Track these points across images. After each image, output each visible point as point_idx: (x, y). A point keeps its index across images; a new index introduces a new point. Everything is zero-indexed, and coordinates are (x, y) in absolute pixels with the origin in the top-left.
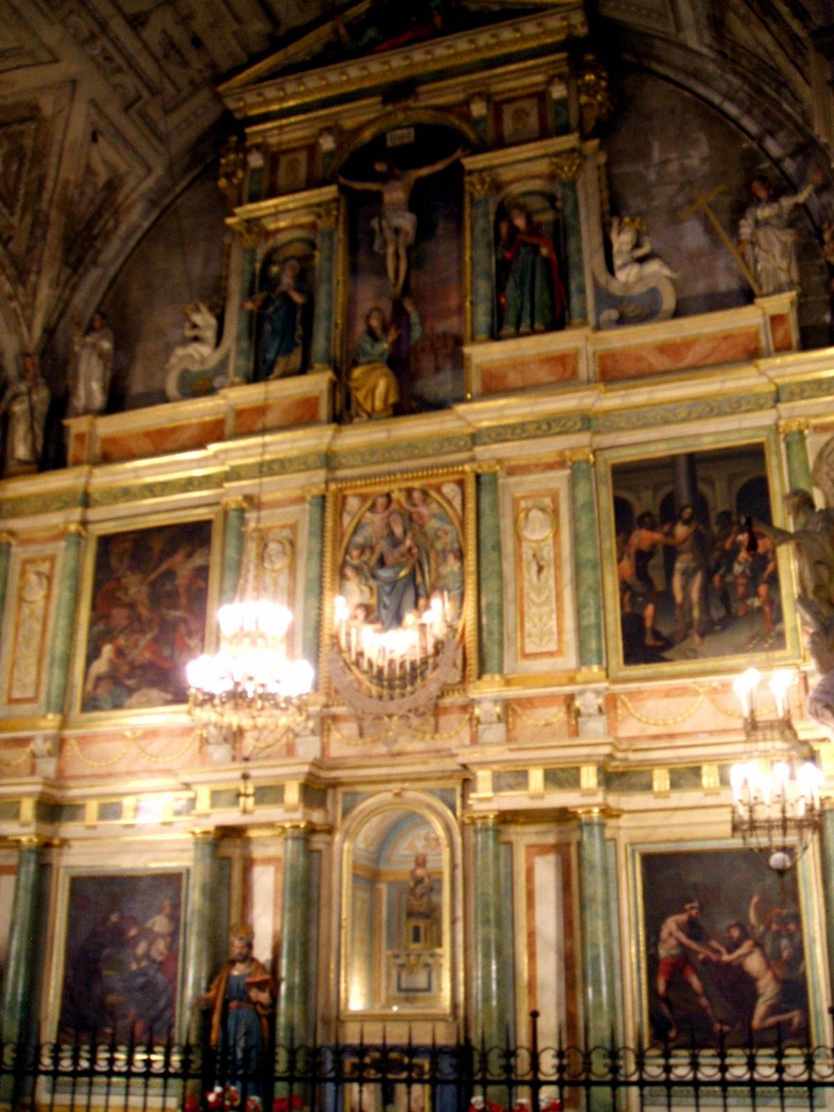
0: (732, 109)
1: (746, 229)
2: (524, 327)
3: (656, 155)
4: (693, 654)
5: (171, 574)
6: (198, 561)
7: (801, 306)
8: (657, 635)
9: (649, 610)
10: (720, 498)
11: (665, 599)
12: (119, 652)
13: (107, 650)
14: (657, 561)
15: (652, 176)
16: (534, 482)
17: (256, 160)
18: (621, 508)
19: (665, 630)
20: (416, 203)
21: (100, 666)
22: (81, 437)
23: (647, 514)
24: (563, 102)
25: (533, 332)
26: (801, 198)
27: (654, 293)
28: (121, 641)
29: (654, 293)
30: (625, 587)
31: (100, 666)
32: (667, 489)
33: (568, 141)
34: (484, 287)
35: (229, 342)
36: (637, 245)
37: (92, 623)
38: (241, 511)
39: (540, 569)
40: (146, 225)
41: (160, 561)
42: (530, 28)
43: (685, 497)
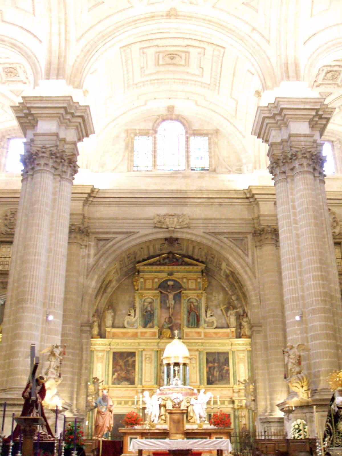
0: (227, 289)
1: (229, 314)
2: (193, 326)
3: (214, 294)
4: (217, 384)
5: (128, 361)
6: (133, 359)
7: (236, 330)
8: (212, 380)
9: (211, 377)
10: (222, 360)
11: (213, 375)
12: (119, 374)
13: (116, 374)
14: (212, 369)
15: (213, 299)
18: (207, 359)
19: (213, 380)
20: (174, 298)
21: (115, 376)
22: (109, 332)
23: (211, 361)
24: (199, 282)
25: (194, 328)
26: (237, 310)
27: (213, 322)
28: (119, 372)
29: (213, 322)
30: (207, 372)
32: (214, 357)
33: (201, 291)
34: (185, 317)
35: (136, 317)
36: (211, 313)
37: (113, 368)
38: (142, 351)
39: (194, 368)
40: (116, 287)
41: (125, 359)
42: (195, 268)
43: (217, 359)
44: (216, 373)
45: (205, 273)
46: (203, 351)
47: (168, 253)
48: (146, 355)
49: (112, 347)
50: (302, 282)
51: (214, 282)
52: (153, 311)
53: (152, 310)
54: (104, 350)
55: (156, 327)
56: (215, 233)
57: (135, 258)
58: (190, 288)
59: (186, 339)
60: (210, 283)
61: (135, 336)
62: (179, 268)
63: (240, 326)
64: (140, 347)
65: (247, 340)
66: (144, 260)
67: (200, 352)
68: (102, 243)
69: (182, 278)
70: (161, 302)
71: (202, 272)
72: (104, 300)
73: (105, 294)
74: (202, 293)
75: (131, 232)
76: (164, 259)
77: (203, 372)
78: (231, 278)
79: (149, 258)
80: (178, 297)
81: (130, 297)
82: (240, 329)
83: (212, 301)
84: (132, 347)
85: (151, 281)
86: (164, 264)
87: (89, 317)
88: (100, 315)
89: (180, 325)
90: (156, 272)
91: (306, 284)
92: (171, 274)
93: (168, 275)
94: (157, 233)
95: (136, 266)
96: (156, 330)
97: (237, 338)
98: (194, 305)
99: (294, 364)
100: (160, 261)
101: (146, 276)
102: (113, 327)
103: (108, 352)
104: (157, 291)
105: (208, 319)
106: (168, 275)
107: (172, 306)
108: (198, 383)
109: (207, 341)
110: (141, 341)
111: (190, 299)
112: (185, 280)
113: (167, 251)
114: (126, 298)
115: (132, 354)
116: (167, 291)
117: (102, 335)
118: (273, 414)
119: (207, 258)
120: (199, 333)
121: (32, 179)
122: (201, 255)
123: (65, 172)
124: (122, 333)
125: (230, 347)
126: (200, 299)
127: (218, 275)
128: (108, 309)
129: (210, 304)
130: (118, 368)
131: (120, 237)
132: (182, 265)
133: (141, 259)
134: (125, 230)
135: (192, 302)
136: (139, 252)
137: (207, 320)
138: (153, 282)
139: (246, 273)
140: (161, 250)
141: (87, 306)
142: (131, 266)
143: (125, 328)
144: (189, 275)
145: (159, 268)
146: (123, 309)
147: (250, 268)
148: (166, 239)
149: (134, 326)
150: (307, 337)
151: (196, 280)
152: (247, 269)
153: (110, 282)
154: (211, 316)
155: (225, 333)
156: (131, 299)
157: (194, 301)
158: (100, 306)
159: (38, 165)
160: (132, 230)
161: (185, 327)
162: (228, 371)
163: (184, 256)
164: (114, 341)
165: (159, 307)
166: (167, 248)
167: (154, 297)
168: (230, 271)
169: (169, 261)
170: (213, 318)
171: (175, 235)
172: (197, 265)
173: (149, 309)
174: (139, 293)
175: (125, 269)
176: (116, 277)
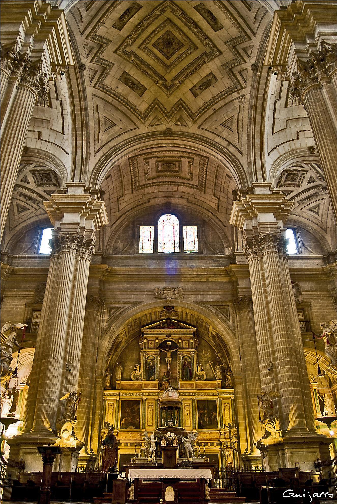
5: (134, 408)
10: (211, 407)
12: (126, 420)
16: (187, 401)
17: (146, 341)
20: (171, 356)
21: (123, 422)
24: (192, 342)
31: (123, 422)
33: (193, 350)
35: (141, 372)
44: (206, 419)
45: (196, 335)
46: (195, 400)
47: (167, 319)
48: (148, 403)
49: (121, 397)
50: (272, 340)
51: (203, 342)
52: (155, 367)
53: (154, 365)
54: (115, 400)
55: (157, 380)
56: (203, 303)
57: (140, 323)
58: (184, 347)
59: (181, 390)
60: (200, 343)
61: (140, 387)
62: (175, 331)
63: (224, 379)
64: (144, 397)
65: (231, 391)
66: (147, 325)
67: (193, 401)
68: (113, 311)
69: (178, 339)
70: (161, 359)
71: (194, 334)
72: (114, 358)
73: (117, 353)
74: (194, 351)
75: (136, 302)
76: (163, 323)
77: (195, 418)
78: (217, 339)
79: (151, 324)
80: (174, 356)
81: (136, 355)
82: (225, 381)
83: (202, 358)
84: (137, 397)
85: (153, 342)
86: (164, 328)
87: (102, 371)
88: (112, 370)
89: (176, 378)
90: (157, 334)
91: (275, 342)
92: (169, 335)
93: (167, 337)
94: (157, 303)
95: (141, 330)
96: (157, 382)
97: (222, 388)
98: (187, 361)
99: (267, 408)
100: (160, 325)
101: (150, 337)
102: (122, 379)
103: (118, 401)
104: (158, 350)
105: (199, 373)
106: (167, 337)
107: (170, 363)
108: (192, 428)
109: (198, 391)
110: (145, 391)
111: (184, 356)
112: (180, 341)
113: (167, 317)
114: (133, 356)
115: (138, 403)
116: (165, 350)
117: (113, 387)
118: (253, 453)
119: (197, 323)
120: (192, 385)
121: (58, 259)
122: (193, 320)
123: (84, 253)
124: (129, 385)
125: (217, 397)
126: (193, 357)
127: (207, 337)
128: (119, 365)
129: (200, 360)
130: (126, 414)
131: (128, 305)
132: (177, 328)
133: (145, 324)
134: (132, 300)
135: (186, 359)
136: (143, 318)
137: (198, 374)
138: (154, 343)
139: (229, 335)
140: (161, 316)
141: (101, 362)
142: (137, 329)
143: (132, 380)
144: (184, 337)
145: (159, 331)
146: (130, 365)
147: (231, 330)
148: (164, 307)
149: (139, 379)
150: (277, 385)
151: (189, 341)
152: (229, 331)
153: (120, 342)
154: (201, 370)
155: (213, 384)
156: (137, 357)
157: (188, 358)
158: (111, 364)
159: (63, 247)
160: (138, 300)
161: (180, 379)
162: (216, 416)
163: (179, 321)
164: (123, 391)
165: (159, 363)
166: (165, 315)
167: (155, 355)
168: (216, 333)
169: (168, 326)
170: (203, 371)
171: (171, 305)
172: (190, 328)
173: (151, 364)
174: (144, 352)
175: (132, 332)
176: (126, 338)
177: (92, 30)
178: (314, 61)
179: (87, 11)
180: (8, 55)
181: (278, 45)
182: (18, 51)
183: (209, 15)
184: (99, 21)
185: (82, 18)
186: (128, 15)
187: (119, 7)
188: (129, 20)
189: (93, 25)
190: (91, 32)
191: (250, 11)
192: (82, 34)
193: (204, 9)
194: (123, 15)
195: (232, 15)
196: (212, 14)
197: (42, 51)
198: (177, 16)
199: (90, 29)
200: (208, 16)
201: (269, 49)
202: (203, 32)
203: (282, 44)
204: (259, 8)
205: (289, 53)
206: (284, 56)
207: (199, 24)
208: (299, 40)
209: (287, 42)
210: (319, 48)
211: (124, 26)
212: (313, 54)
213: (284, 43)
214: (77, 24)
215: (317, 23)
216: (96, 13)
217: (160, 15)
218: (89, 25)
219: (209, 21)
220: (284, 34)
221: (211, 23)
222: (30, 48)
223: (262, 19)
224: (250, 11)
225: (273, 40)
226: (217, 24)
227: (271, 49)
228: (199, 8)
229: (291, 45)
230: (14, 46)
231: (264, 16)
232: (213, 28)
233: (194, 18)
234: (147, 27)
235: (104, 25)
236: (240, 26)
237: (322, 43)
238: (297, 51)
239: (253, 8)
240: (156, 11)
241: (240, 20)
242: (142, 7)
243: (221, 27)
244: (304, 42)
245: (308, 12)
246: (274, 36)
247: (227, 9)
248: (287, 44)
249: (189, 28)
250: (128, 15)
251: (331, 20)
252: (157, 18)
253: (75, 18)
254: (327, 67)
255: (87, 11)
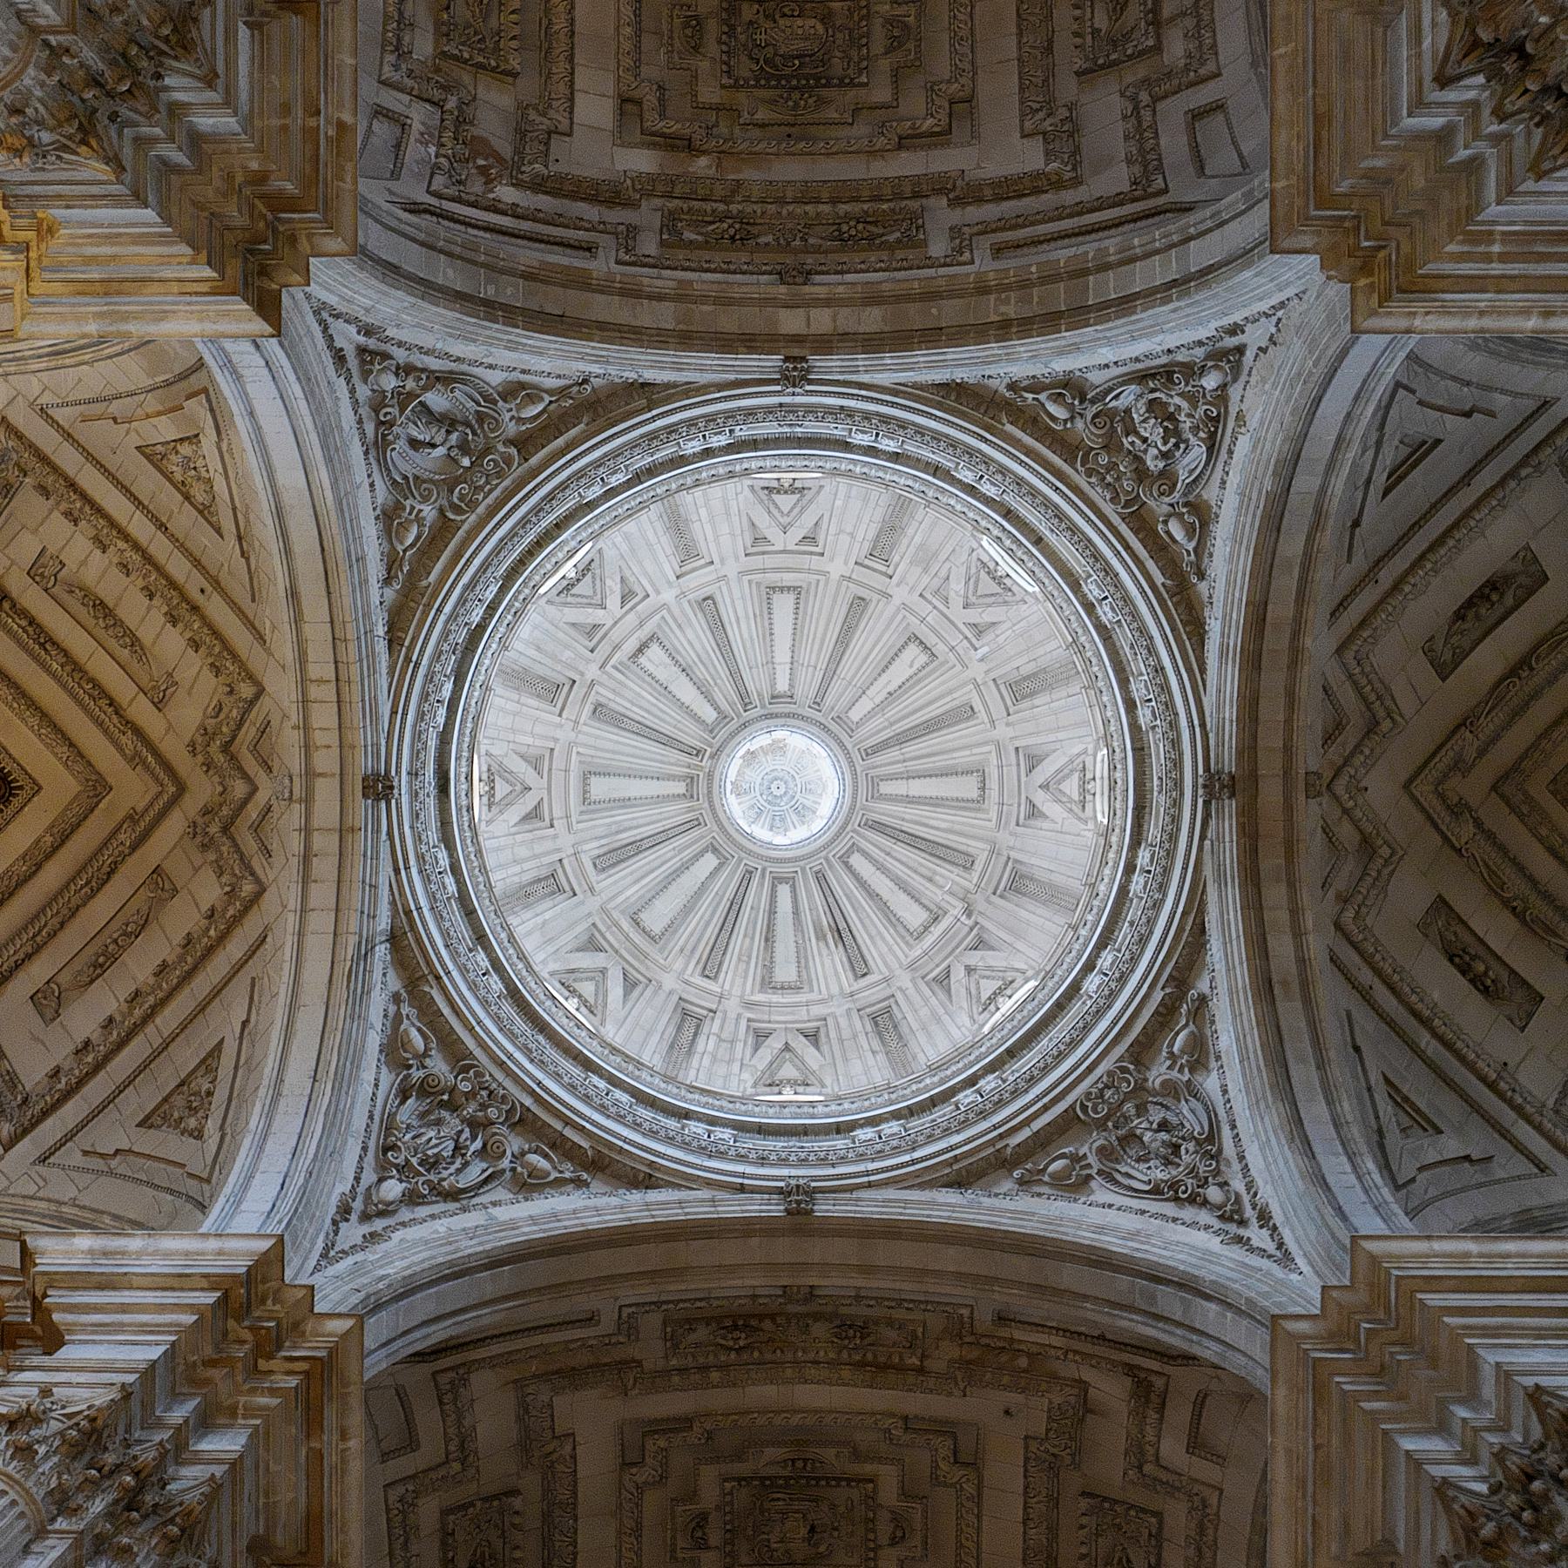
177: (1529, 1121)
178: (1526, 91)
179: (1441, 1132)
180: (1487, 1544)
181: (1501, 284)
182: (1482, 1488)
183: (1471, 614)
184: (1492, 1086)
185: (1467, 1158)
186: (1474, 957)
187: (1436, 995)
188: (1499, 958)
189: (1508, 1116)
190: (1539, 1128)
191: (1438, 442)
192: (1542, 1168)
193: (1448, 636)
194: (1471, 981)
195: (1467, 514)
196: (1470, 603)
197: (1505, 1376)
198: (1482, 752)
199: (1523, 1131)
200: (1478, 617)
201: (1532, 323)
202: (1552, 634)
203: (1497, 269)
204: (1420, 403)
205: (1532, 223)
206: (1551, 242)
207: (1515, 652)
208: (1469, 196)
209: (1481, 249)
210: (1473, 88)
211: (1524, 982)
212: (1501, 115)
213: (1487, 258)
214: (1498, 1182)
215: (1386, 136)
216: (1454, 1096)
217: (1478, 823)
218: (1504, 1133)
219: (1499, 610)
220: (1449, 268)
221: (1509, 600)
222: (1488, 1429)
223: (1468, 384)
224: (1438, 442)
225: (1482, 313)
226: (1515, 575)
227: (1526, 312)
228: (1448, 656)
229: (1494, 223)
230: (1454, 1499)
231: (1454, 378)
232: (1531, 592)
233: (1491, 678)
234: (1532, 880)
235: (1511, 1065)
236: (1512, 474)
237: (1443, 81)
238: (1508, 190)
239: (1423, 429)
240: (1459, 838)
241: (1486, 479)
242: (1440, 896)
243: (1528, 557)
244: (1474, 166)
245: (1343, 187)
246: (1467, 315)
247: (1439, 542)
248: (1492, 242)
249: (1535, 695)
250: (1474, 957)
251: (1374, 76)
252: (1490, 836)
253: (1463, 1190)
254: (1543, 20)
255: (1441, 1132)
